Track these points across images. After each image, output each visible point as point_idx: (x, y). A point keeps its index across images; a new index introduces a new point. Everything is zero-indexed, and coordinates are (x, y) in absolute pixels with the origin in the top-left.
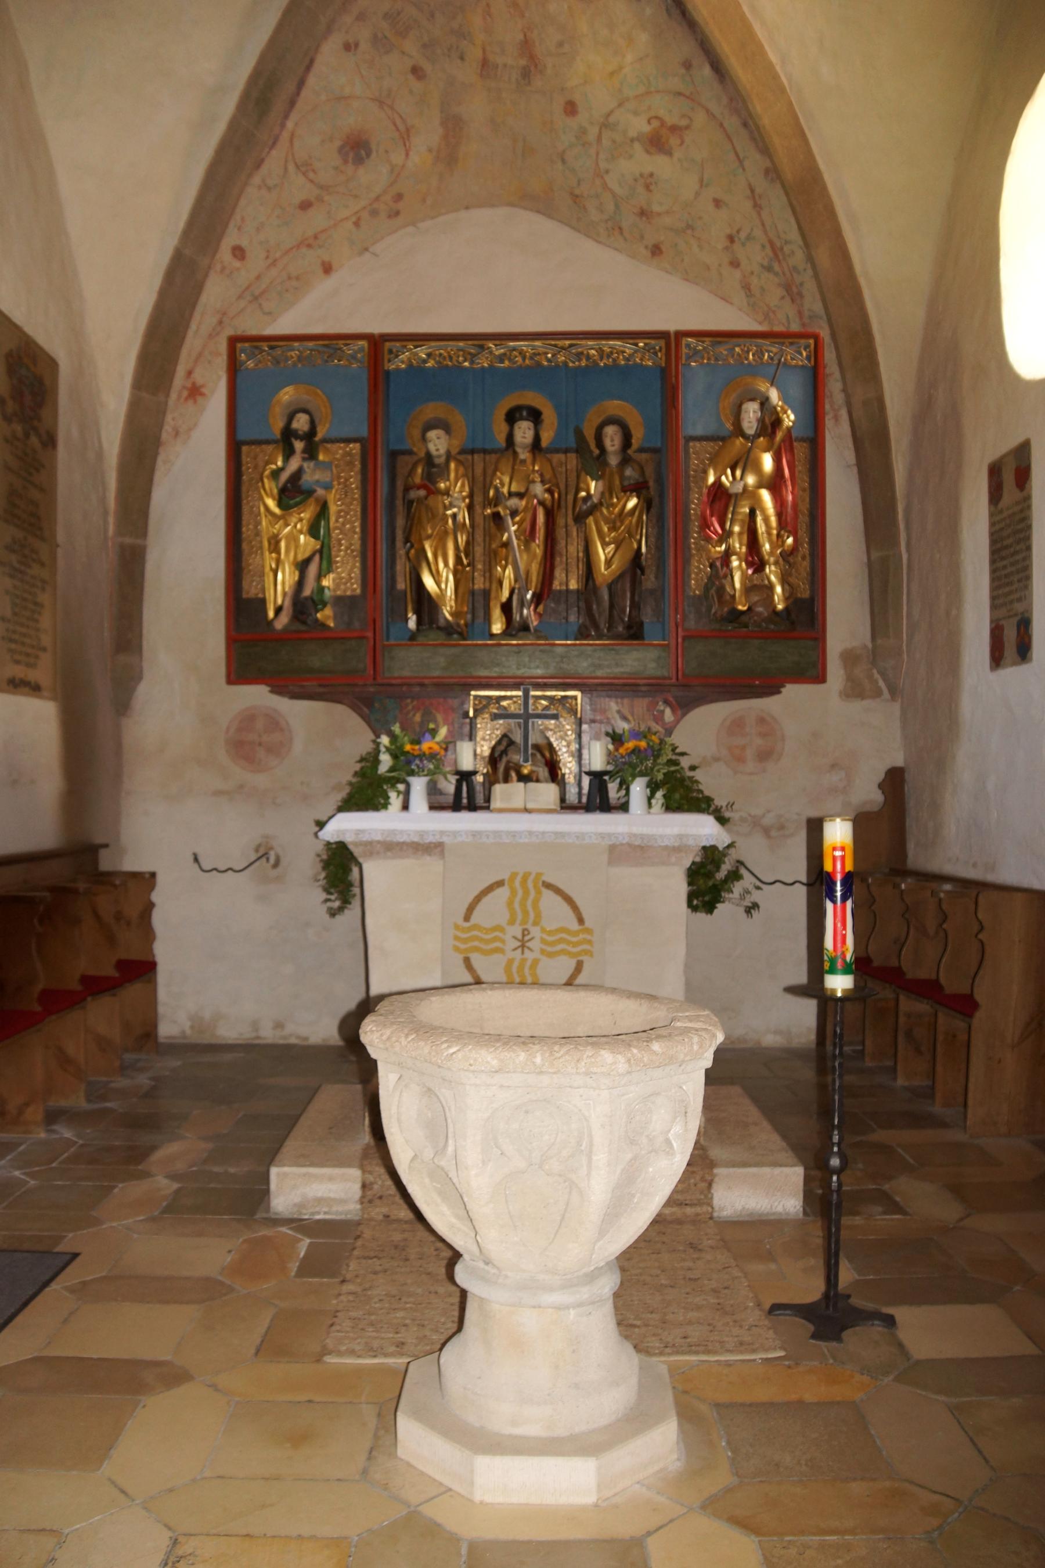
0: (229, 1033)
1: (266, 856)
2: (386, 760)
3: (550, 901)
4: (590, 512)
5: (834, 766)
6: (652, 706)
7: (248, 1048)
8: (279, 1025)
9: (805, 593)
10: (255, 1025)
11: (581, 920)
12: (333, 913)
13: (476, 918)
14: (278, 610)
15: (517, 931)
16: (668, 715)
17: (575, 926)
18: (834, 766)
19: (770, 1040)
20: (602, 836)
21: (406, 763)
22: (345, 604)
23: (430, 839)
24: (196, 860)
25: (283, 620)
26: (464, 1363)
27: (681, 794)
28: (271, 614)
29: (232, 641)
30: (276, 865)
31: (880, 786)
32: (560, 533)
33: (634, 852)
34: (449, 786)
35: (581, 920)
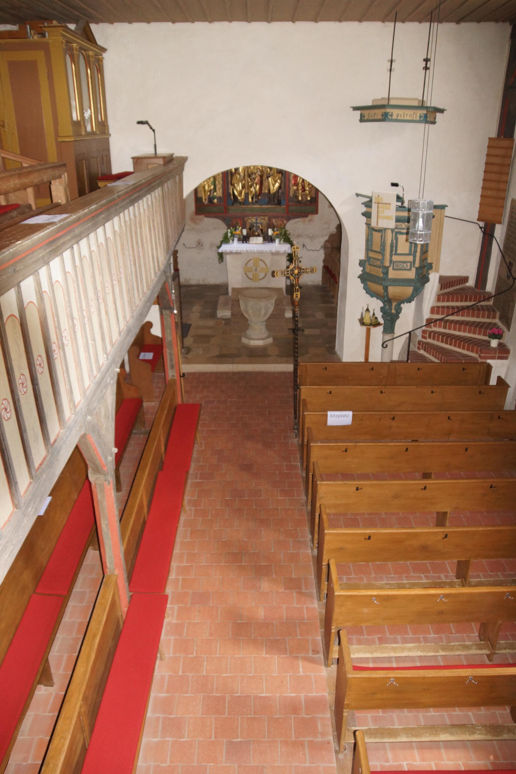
0: (193, 282)
1: (199, 244)
2: (229, 234)
3: (261, 262)
4: (269, 177)
5: (326, 223)
6: (282, 220)
7: (198, 286)
8: (204, 280)
9: (314, 196)
10: (198, 280)
11: (266, 266)
12: (220, 263)
13: (247, 266)
14: (205, 200)
15: (255, 268)
16: (285, 222)
17: (265, 267)
18: (326, 223)
19: (310, 283)
20: (270, 251)
21: (233, 235)
22: (219, 199)
23: (239, 252)
24: (184, 245)
25: (206, 202)
26: (249, 332)
27: (287, 240)
28: (204, 201)
29: (196, 206)
30: (202, 245)
31: (336, 228)
32: (264, 181)
33: (277, 253)
34: (242, 237)
35: (266, 266)
